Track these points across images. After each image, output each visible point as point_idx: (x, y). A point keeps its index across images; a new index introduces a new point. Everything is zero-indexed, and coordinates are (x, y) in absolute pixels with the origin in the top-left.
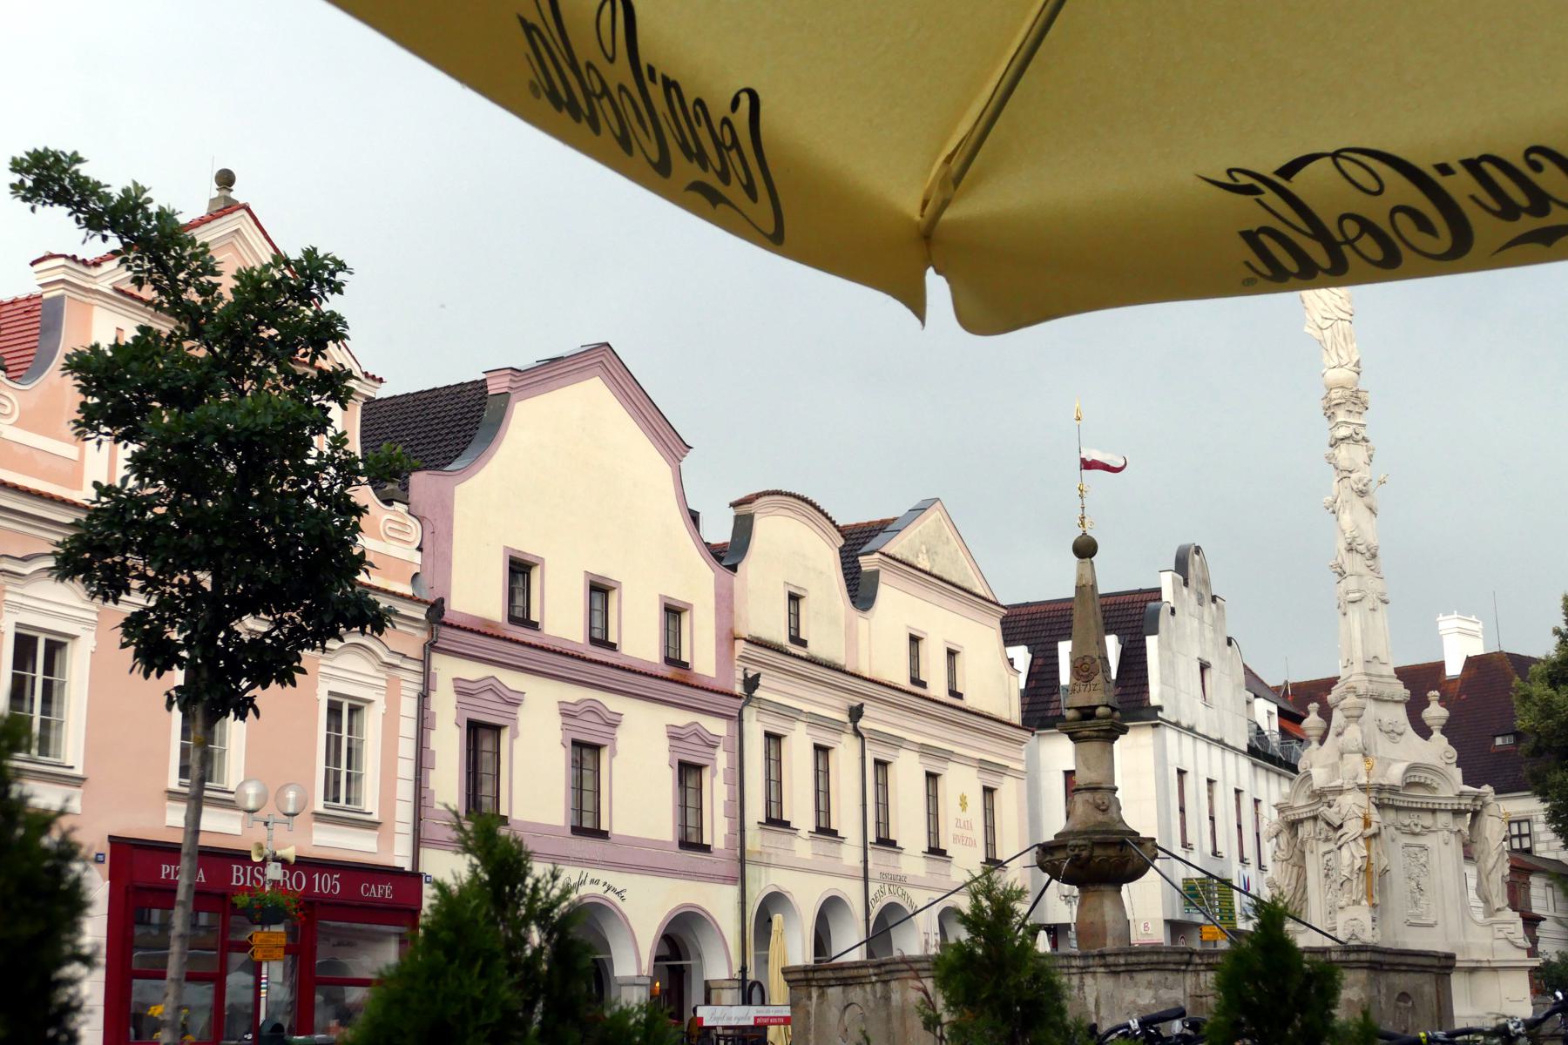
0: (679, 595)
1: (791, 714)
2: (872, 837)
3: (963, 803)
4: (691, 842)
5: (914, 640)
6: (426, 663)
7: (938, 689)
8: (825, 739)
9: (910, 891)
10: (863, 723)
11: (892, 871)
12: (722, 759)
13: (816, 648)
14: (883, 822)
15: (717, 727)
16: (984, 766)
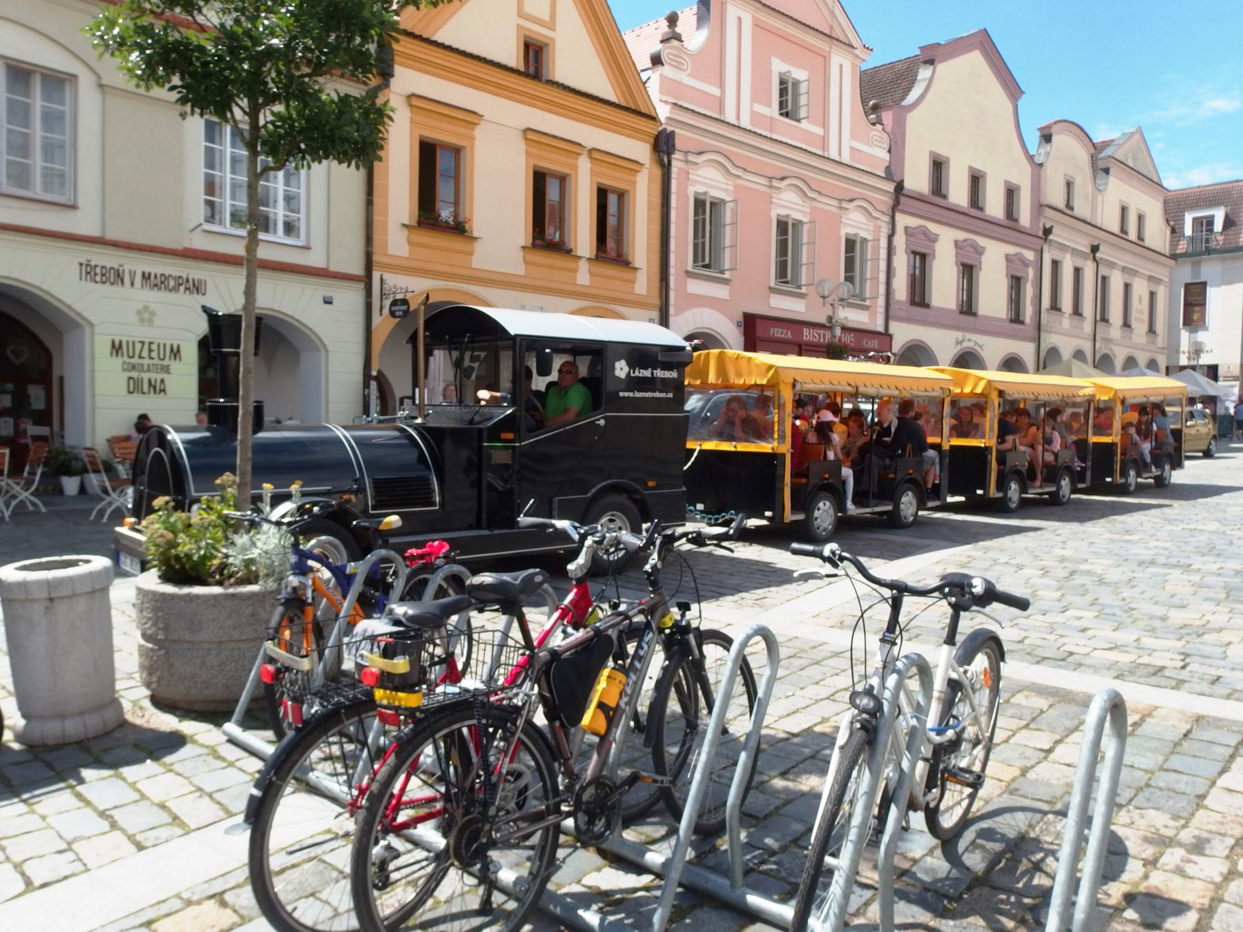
0: (1015, 180)
1: (1063, 248)
2: (1098, 318)
3: (1140, 301)
4: (1016, 319)
5: (1124, 210)
6: (893, 218)
7: (1133, 235)
8: (1080, 263)
9: (1114, 347)
10: (1098, 255)
11: (1106, 336)
12: (1031, 273)
13: (1078, 211)
14: (1017, 313)
15: (1030, 255)
16: (1150, 278)
